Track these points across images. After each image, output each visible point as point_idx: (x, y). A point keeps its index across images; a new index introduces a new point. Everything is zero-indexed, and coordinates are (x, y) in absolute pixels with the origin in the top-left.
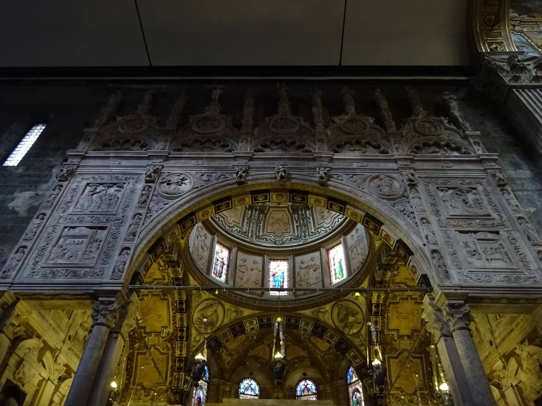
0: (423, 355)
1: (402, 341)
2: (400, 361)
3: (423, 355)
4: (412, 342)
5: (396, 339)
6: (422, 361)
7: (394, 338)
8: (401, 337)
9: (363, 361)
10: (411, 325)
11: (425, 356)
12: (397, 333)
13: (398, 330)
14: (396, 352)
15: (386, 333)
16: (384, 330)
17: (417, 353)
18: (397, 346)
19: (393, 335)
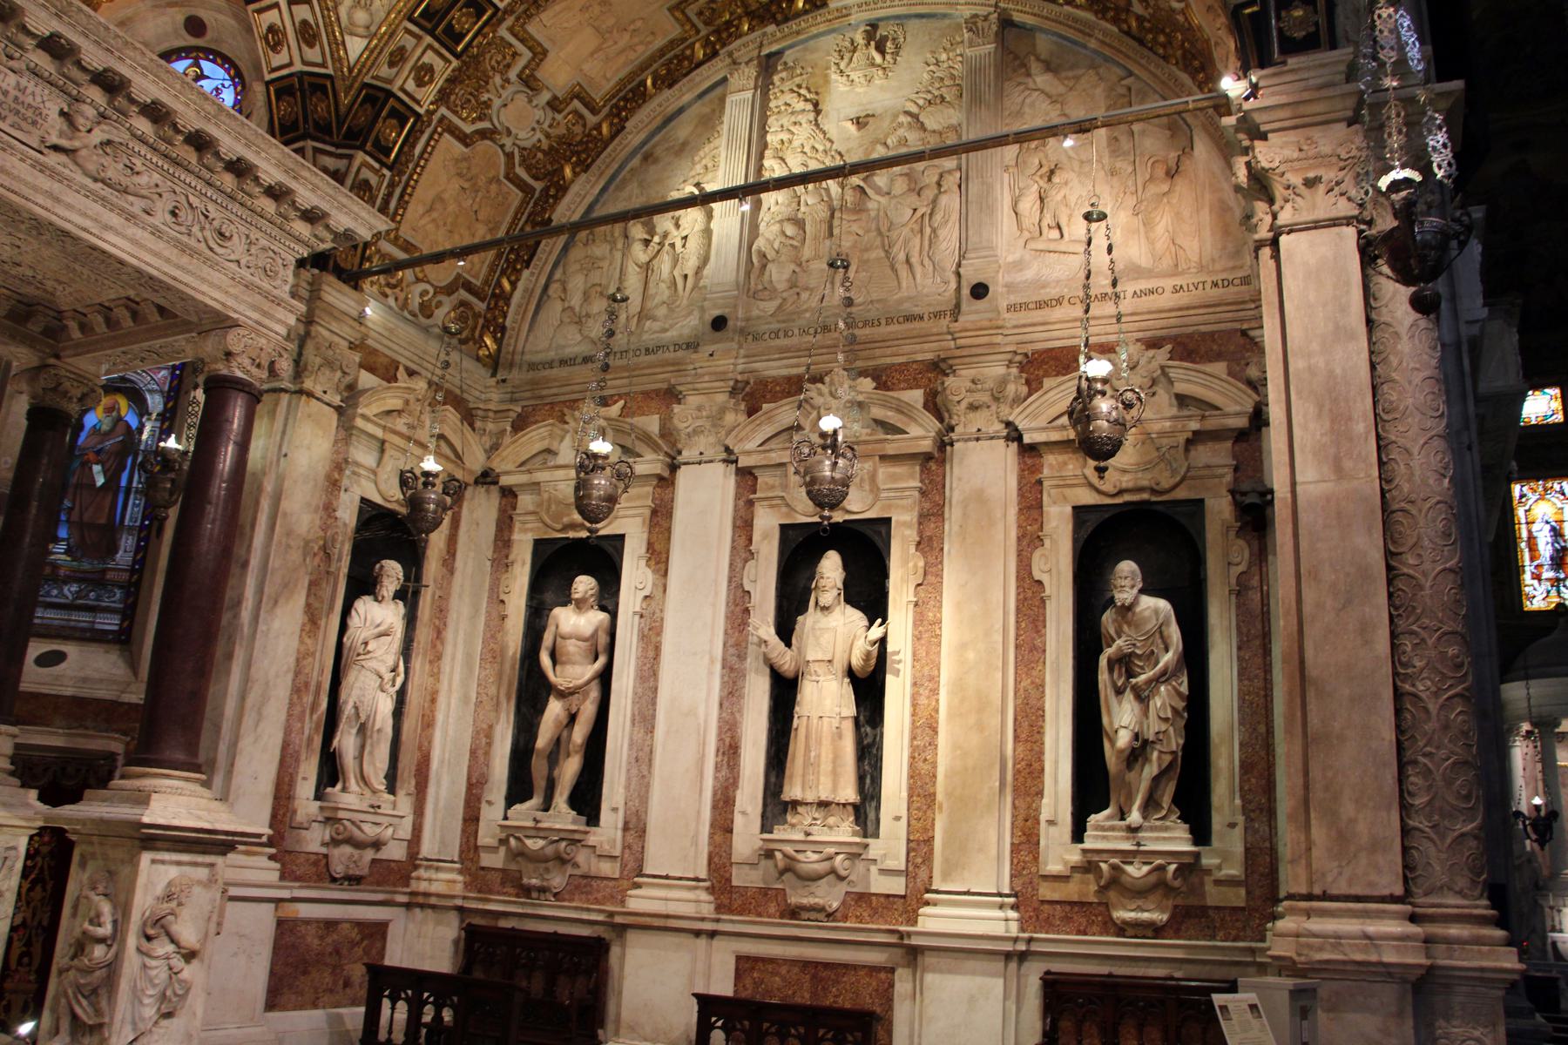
0: (538, 186)
1: (521, 100)
2: (465, 159)
3: (538, 186)
4: (545, 126)
5: (513, 74)
6: (524, 203)
7: (508, 66)
8: (530, 82)
9: (330, 71)
10: (593, 68)
11: (546, 190)
12: (533, 59)
13: (545, 53)
14: (480, 119)
15: (503, 32)
16: (512, 12)
17: (528, 169)
18: (497, 103)
19: (515, 55)
